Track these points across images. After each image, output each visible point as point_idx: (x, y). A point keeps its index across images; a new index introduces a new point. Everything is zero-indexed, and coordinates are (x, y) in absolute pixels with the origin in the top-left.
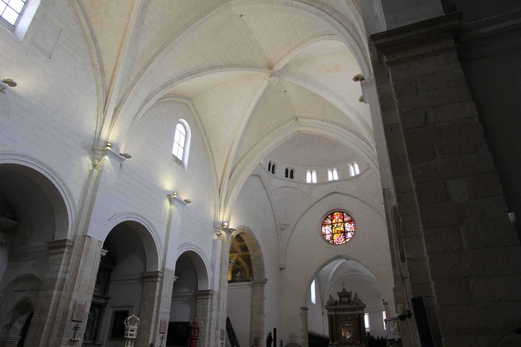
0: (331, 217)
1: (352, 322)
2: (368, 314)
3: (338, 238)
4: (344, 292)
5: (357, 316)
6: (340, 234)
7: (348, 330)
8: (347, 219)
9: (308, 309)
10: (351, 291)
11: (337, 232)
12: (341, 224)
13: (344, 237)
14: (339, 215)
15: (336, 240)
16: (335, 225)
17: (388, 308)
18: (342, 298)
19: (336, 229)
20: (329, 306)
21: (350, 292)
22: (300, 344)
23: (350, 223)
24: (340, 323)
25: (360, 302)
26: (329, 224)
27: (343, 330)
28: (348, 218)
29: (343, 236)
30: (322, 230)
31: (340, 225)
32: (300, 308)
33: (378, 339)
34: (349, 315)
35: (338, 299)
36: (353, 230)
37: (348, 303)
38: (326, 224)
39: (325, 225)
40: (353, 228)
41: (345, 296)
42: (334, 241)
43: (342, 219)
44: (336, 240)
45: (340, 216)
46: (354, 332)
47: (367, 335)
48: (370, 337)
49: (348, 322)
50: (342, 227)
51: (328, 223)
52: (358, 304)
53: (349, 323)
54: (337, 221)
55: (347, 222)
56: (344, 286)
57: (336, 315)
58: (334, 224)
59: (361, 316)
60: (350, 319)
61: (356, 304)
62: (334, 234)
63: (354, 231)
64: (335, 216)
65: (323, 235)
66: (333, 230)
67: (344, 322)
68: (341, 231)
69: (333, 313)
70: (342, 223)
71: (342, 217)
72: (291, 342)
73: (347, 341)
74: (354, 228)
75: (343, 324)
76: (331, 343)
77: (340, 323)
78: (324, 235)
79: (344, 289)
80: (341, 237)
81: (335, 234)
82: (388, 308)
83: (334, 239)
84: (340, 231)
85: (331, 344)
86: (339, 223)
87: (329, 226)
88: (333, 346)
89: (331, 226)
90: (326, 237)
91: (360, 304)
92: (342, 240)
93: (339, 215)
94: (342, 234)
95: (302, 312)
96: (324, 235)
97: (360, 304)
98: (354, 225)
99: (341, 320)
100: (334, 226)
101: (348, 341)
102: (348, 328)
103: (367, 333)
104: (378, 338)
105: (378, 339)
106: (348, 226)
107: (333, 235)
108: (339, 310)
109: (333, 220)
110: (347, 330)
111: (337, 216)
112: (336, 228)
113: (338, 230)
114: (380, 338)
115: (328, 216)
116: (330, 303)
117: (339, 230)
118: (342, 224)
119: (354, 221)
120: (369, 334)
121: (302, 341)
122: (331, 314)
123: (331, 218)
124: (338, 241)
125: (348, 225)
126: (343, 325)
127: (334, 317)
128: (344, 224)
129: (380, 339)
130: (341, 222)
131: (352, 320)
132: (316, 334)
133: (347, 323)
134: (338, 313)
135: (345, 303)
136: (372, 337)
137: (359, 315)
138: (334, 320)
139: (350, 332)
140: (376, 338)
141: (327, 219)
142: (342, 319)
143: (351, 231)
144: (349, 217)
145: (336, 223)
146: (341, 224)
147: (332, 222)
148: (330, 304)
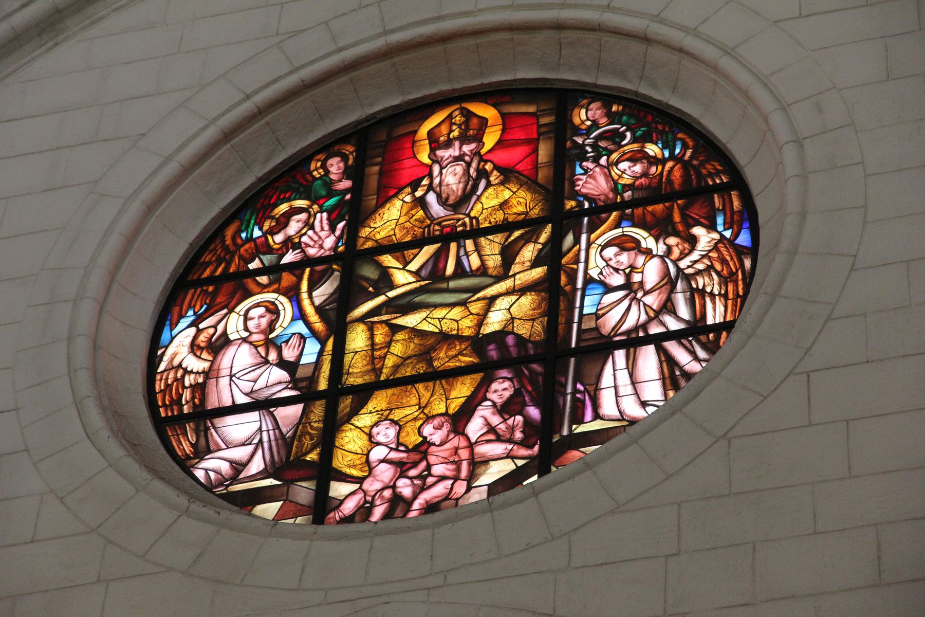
0: (355, 172)
3: (423, 449)
6: (462, 390)
8: (627, 171)
11: (425, 355)
12: (509, 255)
13: (528, 423)
14: (490, 140)
15: (385, 473)
16: (403, 279)
19: (410, 320)
23: (660, 229)
26: (295, 268)
28: (634, 159)
29: (505, 410)
30: (153, 360)
31: (494, 261)
36: (715, 314)
38: (255, 265)
39: (226, 277)
40: (712, 284)
42: (339, 489)
43: (530, 182)
44: (371, 486)
45: (499, 144)
50: (522, 291)
51: (290, 257)
54: (437, 210)
55: (609, 207)
58: (388, 260)
62: (363, 394)
63: (727, 326)
64: (424, 157)
65: (160, 425)
66: (357, 339)
68: (499, 336)
70: (531, 226)
71: (544, 152)
74: (725, 281)
78: (181, 420)
80: (475, 428)
81: (379, 401)
83: (341, 461)
84: (478, 342)
86: (476, 233)
87: (293, 294)
89: (322, 293)
90: (203, 450)
92: (478, 464)
93: (490, 140)
94: (501, 390)
96: (181, 420)
98: (744, 239)
100: (385, 281)
106: (624, 259)
107: (346, 403)
109: (384, 200)
111: (445, 154)
112: (405, 305)
113: (444, 338)
115: (300, 163)
117: (467, 326)
118: (528, 252)
119: (738, 183)
123: (357, 190)
124: (405, 488)
125: (625, 244)
128: (556, 240)
130: (505, 227)
141: (284, 208)
143: (673, 325)
144: (652, 149)
145: (418, 243)
146: (509, 255)
147: (352, 234)
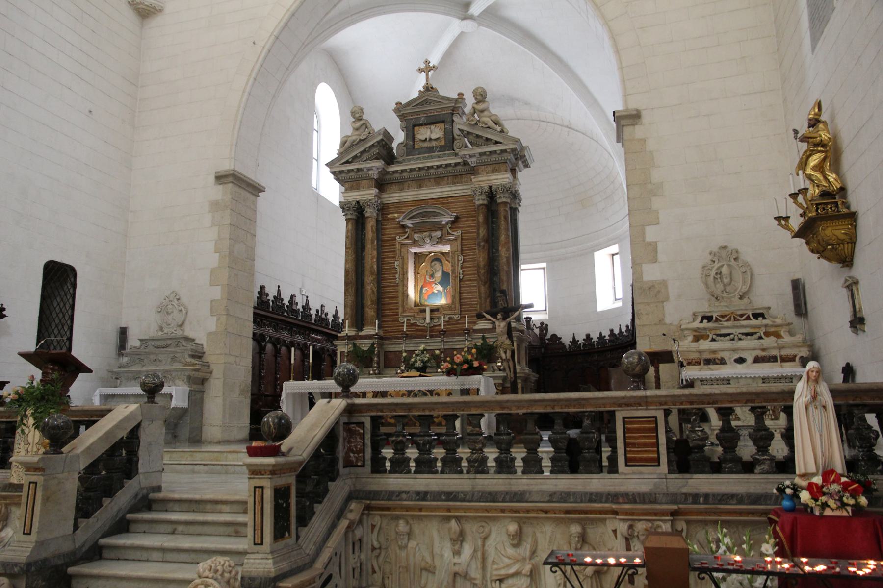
1: (458, 233)
2: (544, 265)
4: (427, 102)
5: (481, 200)
7: (439, 275)
9: (262, 190)
10: (461, 94)
17: (644, 141)
18: (416, 129)
20: (347, 162)
21: (456, 97)
22: (200, 337)
24: (399, 239)
25: (499, 129)
27: (416, 273)
32: (212, 179)
33: (574, 341)
34: (444, 202)
35: (399, 137)
37: (442, 148)
41: (432, 122)
46: (461, 280)
47: (537, 331)
48: (548, 336)
49: (439, 234)
52: (487, 139)
53: (441, 240)
56: (430, 73)
57: (383, 209)
59: (502, 198)
60: (445, 220)
61: (477, 140)
67: (416, 236)
69: (368, 194)
72: (160, 333)
73: (428, 320)
75: (415, 243)
76: (347, 331)
77: (399, 239)
79: (428, 89)
82: (644, 141)
85: (349, 338)
88: (354, 345)
91: (497, 142)
95: (218, 193)
97: (497, 142)
99: (404, 227)
101: (431, 319)
102: (437, 265)
103: (538, 325)
104: (574, 337)
105: (574, 341)
108: (401, 182)
110: (432, 276)
114: (581, 338)
116: (353, 145)
120: (544, 327)
121: (211, 325)
122: (358, 202)
126: (414, 250)
127: (370, 212)
129: (581, 341)
131: (455, 221)
132: (306, 307)
133: (431, 237)
134: (393, 196)
135: (431, 150)
136: (554, 336)
137: (491, 195)
138: (371, 224)
139: (445, 279)
140: (567, 340)
142: (409, 223)
148: (356, 152)
